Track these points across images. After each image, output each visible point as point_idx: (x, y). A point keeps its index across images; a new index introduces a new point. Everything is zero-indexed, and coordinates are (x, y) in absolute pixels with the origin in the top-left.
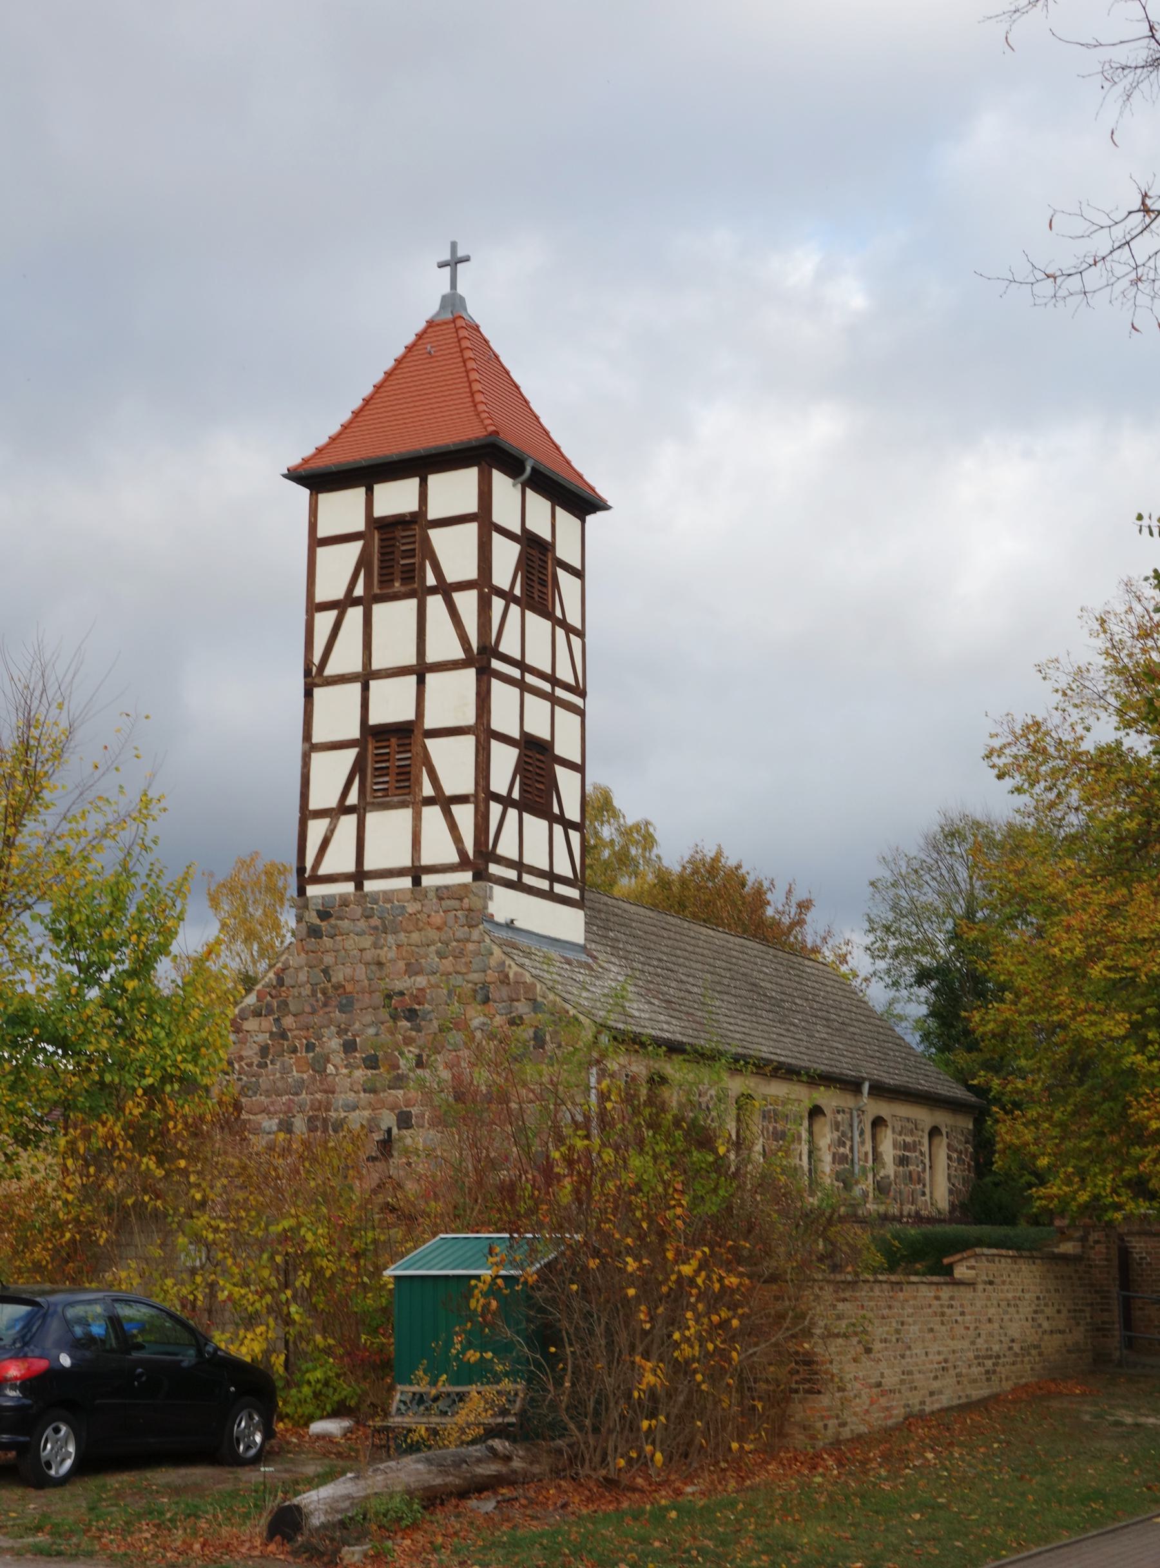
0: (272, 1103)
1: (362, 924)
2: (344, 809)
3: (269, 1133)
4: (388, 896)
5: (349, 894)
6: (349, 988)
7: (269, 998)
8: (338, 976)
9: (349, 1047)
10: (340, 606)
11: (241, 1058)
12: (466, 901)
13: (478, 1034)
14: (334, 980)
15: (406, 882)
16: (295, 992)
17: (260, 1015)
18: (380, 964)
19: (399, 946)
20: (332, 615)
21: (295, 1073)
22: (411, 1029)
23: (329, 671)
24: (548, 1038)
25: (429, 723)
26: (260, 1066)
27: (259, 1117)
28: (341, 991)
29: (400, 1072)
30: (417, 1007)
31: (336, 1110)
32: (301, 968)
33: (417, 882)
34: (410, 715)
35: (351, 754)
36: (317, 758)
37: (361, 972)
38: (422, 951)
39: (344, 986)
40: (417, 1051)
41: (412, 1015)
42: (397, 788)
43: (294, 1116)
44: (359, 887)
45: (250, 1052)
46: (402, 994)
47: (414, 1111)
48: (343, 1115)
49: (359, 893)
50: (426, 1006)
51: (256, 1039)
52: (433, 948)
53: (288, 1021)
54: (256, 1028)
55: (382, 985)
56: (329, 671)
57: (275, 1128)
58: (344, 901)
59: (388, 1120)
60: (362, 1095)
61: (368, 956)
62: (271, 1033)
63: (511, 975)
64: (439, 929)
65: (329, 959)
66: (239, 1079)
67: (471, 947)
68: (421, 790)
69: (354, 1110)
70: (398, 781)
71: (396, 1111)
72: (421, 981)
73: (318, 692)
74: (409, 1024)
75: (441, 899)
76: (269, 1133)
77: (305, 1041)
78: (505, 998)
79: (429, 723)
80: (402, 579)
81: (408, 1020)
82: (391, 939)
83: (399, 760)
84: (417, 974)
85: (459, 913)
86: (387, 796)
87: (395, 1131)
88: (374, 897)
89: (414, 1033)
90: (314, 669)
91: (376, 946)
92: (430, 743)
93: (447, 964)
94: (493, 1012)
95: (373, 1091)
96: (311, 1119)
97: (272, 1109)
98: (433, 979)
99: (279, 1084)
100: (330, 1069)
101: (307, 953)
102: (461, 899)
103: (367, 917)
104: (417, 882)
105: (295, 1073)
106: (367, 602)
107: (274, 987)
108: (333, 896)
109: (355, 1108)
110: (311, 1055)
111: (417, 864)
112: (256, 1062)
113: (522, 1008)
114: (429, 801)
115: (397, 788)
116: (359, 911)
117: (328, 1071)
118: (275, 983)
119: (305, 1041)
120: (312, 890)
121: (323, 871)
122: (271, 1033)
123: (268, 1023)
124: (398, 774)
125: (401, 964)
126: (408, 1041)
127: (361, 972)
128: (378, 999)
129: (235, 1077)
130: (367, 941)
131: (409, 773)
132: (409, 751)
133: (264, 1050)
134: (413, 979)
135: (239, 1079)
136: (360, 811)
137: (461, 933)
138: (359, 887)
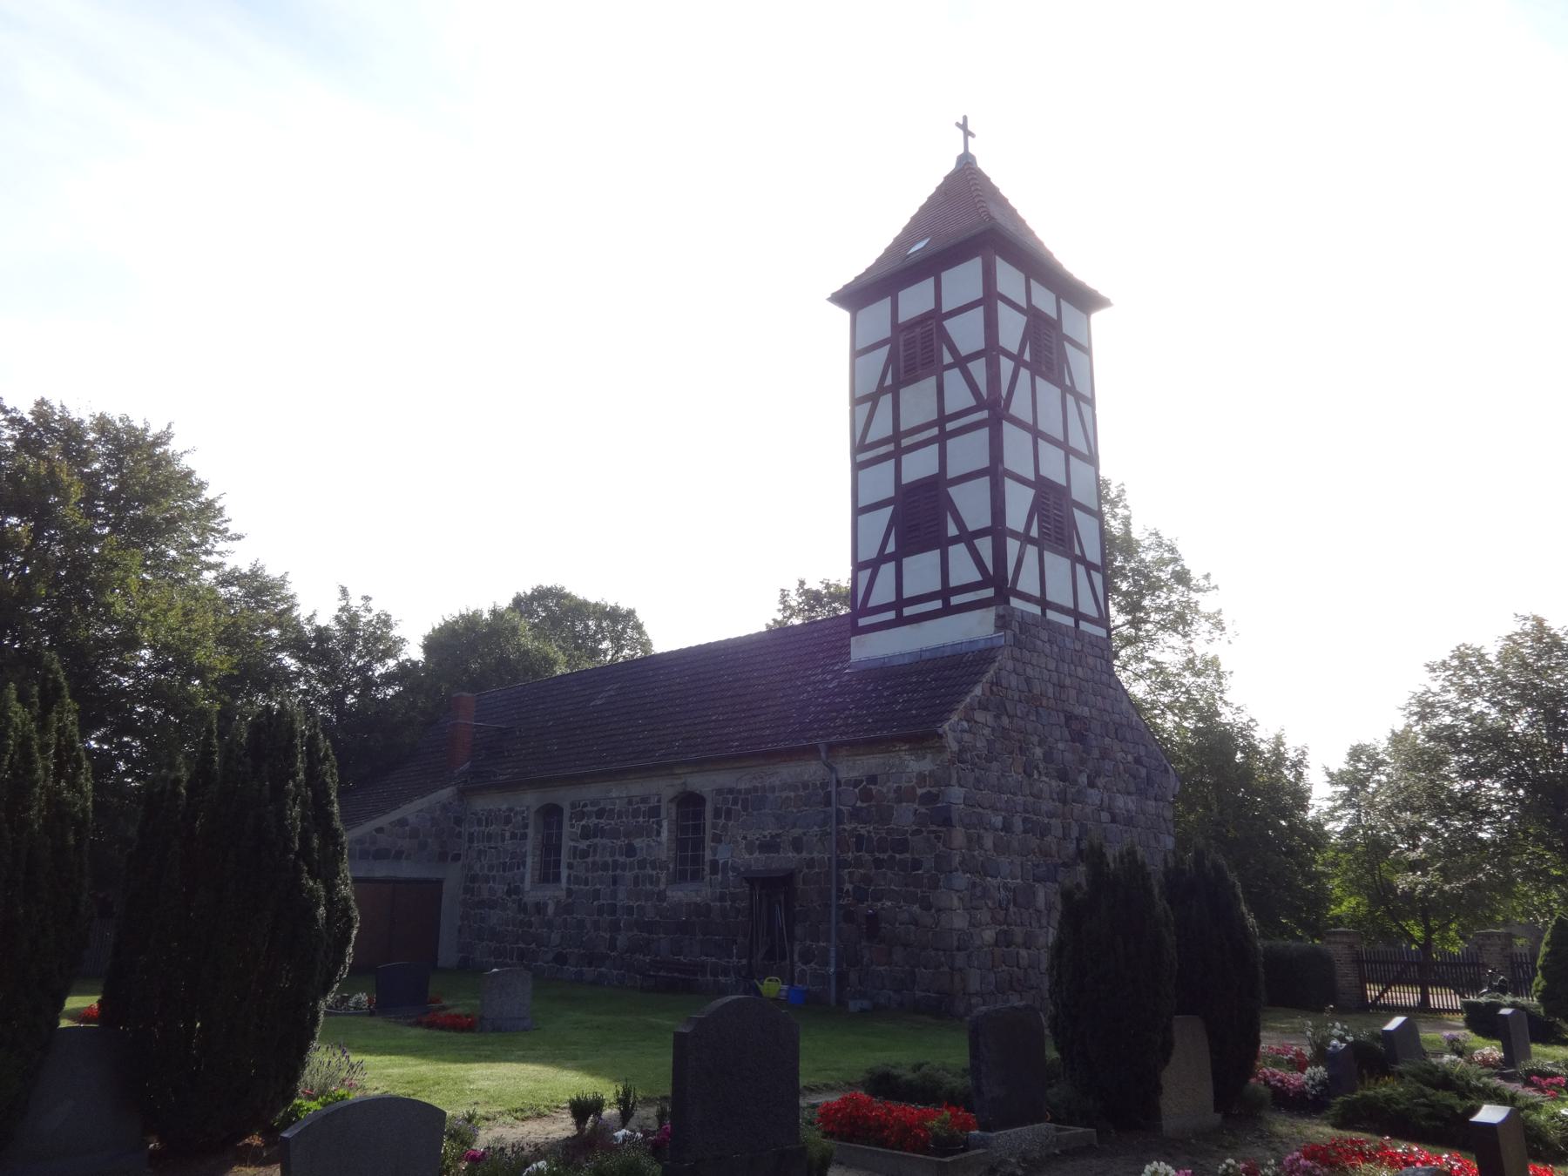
30: (1085, 733)
72: (1086, 711)
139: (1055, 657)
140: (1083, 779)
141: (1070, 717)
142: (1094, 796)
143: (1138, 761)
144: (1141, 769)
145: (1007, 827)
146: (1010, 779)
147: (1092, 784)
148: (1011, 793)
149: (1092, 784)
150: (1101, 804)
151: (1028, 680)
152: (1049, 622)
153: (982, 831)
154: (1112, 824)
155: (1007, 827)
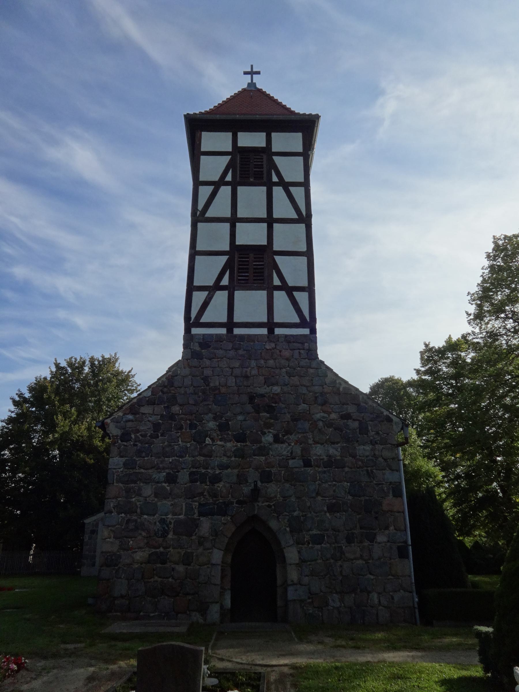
0: (162, 462)
1: (232, 353)
2: (217, 287)
3: (158, 482)
4: (250, 337)
5: (223, 334)
6: (223, 390)
7: (160, 393)
8: (215, 382)
9: (223, 427)
10: (217, 185)
11: (138, 431)
12: (306, 344)
13: (321, 424)
14: (212, 385)
15: (264, 331)
16: (182, 391)
17: (154, 404)
18: (247, 377)
19: (259, 367)
20: (212, 188)
21: (180, 443)
22: (270, 418)
23: (208, 214)
24: (370, 428)
25: (276, 248)
26: (151, 436)
27: (150, 471)
28: (217, 392)
29: (262, 444)
30: (274, 405)
31: (213, 468)
32: (186, 376)
33: (271, 331)
34: (265, 243)
35: (224, 259)
36: (198, 259)
37: (231, 381)
38: (277, 371)
39: (219, 389)
40: (275, 432)
41: (270, 409)
42: (254, 280)
43: (178, 472)
44: (230, 331)
45: (146, 427)
46: (263, 396)
47: (273, 470)
48: (218, 472)
49: (230, 335)
50: (281, 404)
51: (150, 419)
52: (284, 370)
53: (176, 409)
54: (151, 412)
55: (249, 390)
56: (208, 214)
57: (162, 479)
58: (219, 338)
59: (253, 476)
60: (233, 459)
61: (237, 372)
62: (162, 416)
63: (341, 389)
64: (288, 359)
65: (208, 372)
66: (135, 445)
67: (311, 371)
68: (273, 281)
69: (227, 469)
70: (254, 276)
71: (260, 471)
72: (277, 389)
73: (200, 225)
74: (268, 415)
75: (289, 342)
76: (158, 482)
77: (188, 422)
78: (339, 403)
79: (276, 248)
80: (255, 178)
81: (268, 412)
82: (253, 363)
83: (255, 265)
84: (273, 385)
85: (302, 351)
86: (247, 283)
87: (259, 484)
88: (242, 337)
89: (273, 421)
90: (198, 213)
91: (242, 366)
92: (277, 258)
93: (295, 380)
94: (331, 411)
95: (243, 457)
96: (191, 474)
97: (161, 466)
98: (285, 389)
99: (167, 449)
100: (208, 441)
101: (190, 367)
102: (303, 344)
103: (236, 349)
104: (271, 331)
105: (180, 443)
106: (234, 185)
107: (165, 387)
108: (211, 335)
109: (227, 467)
110: (194, 431)
111: (271, 321)
112: (149, 434)
113: (351, 409)
114: (278, 288)
115: (254, 280)
116: (230, 345)
117: (207, 442)
118: (166, 384)
119: (188, 422)
120: (195, 331)
121: (203, 320)
122: (162, 416)
123: (159, 409)
124: (254, 273)
125: (262, 378)
126: (268, 426)
127: (231, 381)
128: (245, 398)
129: (132, 443)
130: (237, 364)
131: (263, 272)
132: (263, 261)
133: (156, 426)
134: (270, 387)
135: (135, 445)
136: (231, 290)
137: (303, 363)
138: (230, 331)
139: (240, 358)
140: (269, 438)
141: (252, 398)
142: (283, 449)
143: (347, 417)
144: (350, 422)
145: (171, 479)
146: (176, 447)
147: (277, 440)
148: (177, 457)
149: (277, 440)
150: (292, 453)
151: (206, 379)
152: (236, 336)
153: (142, 484)
154: (307, 469)
155: (171, 479)
